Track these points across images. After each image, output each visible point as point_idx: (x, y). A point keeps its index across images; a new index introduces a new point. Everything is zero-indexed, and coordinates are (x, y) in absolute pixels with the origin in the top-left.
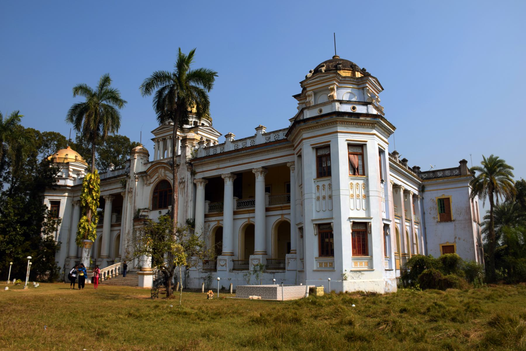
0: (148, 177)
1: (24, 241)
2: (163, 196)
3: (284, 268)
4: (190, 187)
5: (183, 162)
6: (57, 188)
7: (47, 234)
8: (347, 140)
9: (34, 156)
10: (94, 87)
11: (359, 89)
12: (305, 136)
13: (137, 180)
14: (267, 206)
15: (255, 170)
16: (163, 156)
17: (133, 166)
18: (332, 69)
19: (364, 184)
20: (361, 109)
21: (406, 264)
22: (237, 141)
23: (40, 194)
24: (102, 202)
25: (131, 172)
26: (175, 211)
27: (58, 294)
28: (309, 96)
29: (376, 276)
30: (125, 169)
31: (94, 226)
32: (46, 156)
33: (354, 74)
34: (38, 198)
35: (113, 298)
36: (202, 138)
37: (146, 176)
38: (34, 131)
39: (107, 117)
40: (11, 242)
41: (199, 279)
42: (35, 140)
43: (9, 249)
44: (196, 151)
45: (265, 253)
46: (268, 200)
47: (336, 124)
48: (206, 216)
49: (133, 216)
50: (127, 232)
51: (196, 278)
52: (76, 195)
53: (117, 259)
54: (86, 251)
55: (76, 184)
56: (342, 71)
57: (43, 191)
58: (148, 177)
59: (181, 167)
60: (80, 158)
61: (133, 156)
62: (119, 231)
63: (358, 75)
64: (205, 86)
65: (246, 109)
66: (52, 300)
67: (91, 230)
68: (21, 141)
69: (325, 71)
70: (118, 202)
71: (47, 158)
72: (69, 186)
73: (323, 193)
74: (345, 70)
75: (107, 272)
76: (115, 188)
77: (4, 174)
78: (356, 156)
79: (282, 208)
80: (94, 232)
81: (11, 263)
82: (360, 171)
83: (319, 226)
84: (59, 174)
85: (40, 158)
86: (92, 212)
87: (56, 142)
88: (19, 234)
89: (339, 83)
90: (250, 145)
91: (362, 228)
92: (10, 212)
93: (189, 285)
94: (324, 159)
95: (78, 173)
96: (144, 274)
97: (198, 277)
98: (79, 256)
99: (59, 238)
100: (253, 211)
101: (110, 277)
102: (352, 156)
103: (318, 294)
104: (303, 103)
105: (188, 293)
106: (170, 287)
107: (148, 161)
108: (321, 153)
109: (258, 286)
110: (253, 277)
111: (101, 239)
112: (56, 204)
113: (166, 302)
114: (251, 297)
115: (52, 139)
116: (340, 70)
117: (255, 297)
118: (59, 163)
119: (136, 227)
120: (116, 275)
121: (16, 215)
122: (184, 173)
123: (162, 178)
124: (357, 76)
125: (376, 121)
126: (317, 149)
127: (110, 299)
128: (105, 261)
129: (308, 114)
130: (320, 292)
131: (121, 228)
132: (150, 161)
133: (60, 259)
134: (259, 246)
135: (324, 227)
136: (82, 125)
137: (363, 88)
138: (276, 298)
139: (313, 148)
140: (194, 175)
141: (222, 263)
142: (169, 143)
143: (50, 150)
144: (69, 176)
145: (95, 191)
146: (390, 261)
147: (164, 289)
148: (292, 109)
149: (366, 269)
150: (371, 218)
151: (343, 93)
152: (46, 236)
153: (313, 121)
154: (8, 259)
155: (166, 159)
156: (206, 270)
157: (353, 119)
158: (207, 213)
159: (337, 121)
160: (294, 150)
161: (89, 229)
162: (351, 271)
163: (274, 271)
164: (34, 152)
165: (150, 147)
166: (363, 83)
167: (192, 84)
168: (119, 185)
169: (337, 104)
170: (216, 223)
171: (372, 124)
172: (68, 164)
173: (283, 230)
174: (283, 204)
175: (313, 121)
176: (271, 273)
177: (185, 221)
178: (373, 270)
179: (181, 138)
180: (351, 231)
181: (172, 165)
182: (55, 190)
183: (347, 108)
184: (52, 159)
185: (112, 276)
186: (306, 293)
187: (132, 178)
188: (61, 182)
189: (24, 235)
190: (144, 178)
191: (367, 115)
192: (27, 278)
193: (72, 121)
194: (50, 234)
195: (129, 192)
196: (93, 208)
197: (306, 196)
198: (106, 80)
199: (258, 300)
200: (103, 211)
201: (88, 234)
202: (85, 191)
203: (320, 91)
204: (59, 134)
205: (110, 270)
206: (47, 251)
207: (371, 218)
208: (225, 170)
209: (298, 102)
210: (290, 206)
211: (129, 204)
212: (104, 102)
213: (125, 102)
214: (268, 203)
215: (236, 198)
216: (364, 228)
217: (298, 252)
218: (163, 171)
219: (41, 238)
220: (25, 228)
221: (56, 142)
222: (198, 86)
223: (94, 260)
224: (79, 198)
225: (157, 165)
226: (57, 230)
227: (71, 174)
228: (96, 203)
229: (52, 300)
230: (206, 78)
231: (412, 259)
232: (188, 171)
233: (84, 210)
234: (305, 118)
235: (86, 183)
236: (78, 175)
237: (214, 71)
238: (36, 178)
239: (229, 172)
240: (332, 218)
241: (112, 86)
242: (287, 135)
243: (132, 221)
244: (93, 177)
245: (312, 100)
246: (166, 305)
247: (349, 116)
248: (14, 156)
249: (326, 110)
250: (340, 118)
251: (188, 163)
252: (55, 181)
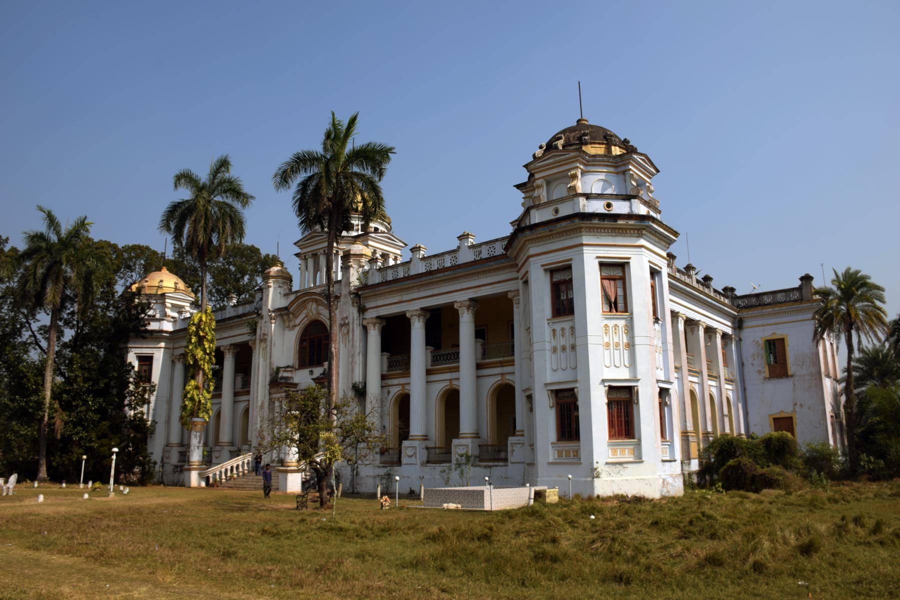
0: (291, 316)
1: (99, 422)
2: (315, 346)
3: (506, 460)
4: (358, 331)
5: (344, 291)
6: (148, 335)
7: (135, 409)
8: (598, 257)
9: (110, 284)
10: (203, 175)
11: (617, 173)
12: (532, 251)
13: (273, 321)
14: (479, 361)
15: (459, 304)
16: (315, 282)
17: (267, 299)
18: (574, 143)
19: (626, 326)
20: (620, 207)
21: (706, 450)
22: (429, 257)
23: (122, 346)
24: (219, 355)
25: (264, 307)
26: (334, 372)
27: (159, 504)
28: (539, 187)
29: (649, 471)
30: (255, 304)
31: (208, 396)
32: (128, 284)
33: (609, 150)
34: (118, 352)
35: (241, 510)
36: (374, 253)
37: (288, 315)
38: (108, 244)
39: (224, 223)
40: (79, 423)
41: (374, 477)
42: (111, 260)
43: (77, 434)
44: (366, 273)
45: (477, 435)
46: (480, 351)
47: (581, 232)
48: (383, 377)
49: (268, 379)
50: (259, 404)
51: (370, 477)
52: (177, 345)
53: (245, 447)
54: (196, 436)
55: (177, 328)
56: (589, 146)
57: (127, 342)
58: (291, 316)
59: (342, 299)
60: (181, 285)
61: (267, 283)
62: (246, 403)
63: (616, 151)
64: (374, 170)
65: (442, 205)
66: (154, 513)
67: (203, 401)
68: (91, 263)
69: (563, 147)
70: (244, 357)
71: (130, 287)
72: (166, 332)
73: (562, 342)
74: (594, 143)
75: (229, 468)
76: (240, 335)
77: (66, 316)
78: (612, 282)
79: (501, 364)
80: (209, 405)
81: (85, 457)
82: (621, 305)
84: (151, 313)
85: (119, 289)
86: (205, 374)
87: (142, 262)
88: (91, 410)
89: (585, 165)
90: (449, 265)
91: (624, 396)
92: (76, 376)
93: (358, 487)
94: (563, 287)
95: (179, 309)
96: (287, 472)
97: (372, 474)
98: (186, 442)
99: (154, 416)
100: (457, 369)
101: (235, 476)
102: (606, 282)
103: (548, 500)
104: (530, 197)
105: (356, 500)
106: (325, 492)
107: (291, 290)
109: (459, 488)
110: (455, 475)
111: (218, 415)
112: (146, 361)
113: (317, 514)
114: (445, 505)
115: (138, 257)
116: (586, 144)
117: (452, 506)
118: (150, 296)
119: (274, 396)
120: (243, 472)
121: (85, 380)
122: (347, 310)
123: (314, 318)
124: (614, 154)
125: (640, 226)
126: (552, 272)
127: (237, 511)
128: (226, 450)
129: (537, 217)
130: (552, 496)
131: (251, 397)
132: (294, 289)
133: (156, 448)
134: (466, 424)
135: (565, 394)
136: (185, 236)
137: (624, 173)
138: (483, 507)
139: (546, 270)
140: (363, 313)
141: (410, 452)
142: (323, 261)
143: (134, 274)
144: (165, 315)
145: (208, 341)
146: (672, 446)
147: (318, 494)
148: (515, 206)
149: (631, 460)
150: (638, 380)
151: (592, 182)
152: (132, 413)
153: (545, 228)
154: (75, 449)
155: (319, 286)
156: (384, 462)
157: (607, 223)
158: (385, 373)
159: (582, 228)
160: (518, 272)
161: (200, 401)
162: (607, 463)
163: (491, 464)
164: (111, 279)
165: (293, 266)
166: (624, 165)
167: (356, 169)
168: (246, 330)
169: (582, 201)
170: (400, 388)
171: (638, 230)
172: (163, 295)
173: (504, 397)
174: (503, 357)
175: (545, 228)
176: (485, 467)
177: (351, 386)
178: (642, 462)
179: (341, 253)
180: (606, 401)
181: (329, 297)
182: (144, 338)
183: (597, 207)
184: (139, 289)
185: (238, 474)
186: (530, 498)
187: (266, 318)
188: (154, 326)
189: (97, 411)
190: (285, 317)
191: (630, 216)
192: (112, 480)
193: (168, 229)
194: (140, 409)
195: (261, 341)
196: (206, 367)
197: (536, 347)
198: (224, 164)
199: (456, 511)
200: (222, 369)
201: (199, 409)
202: (193, 341)
203: (557, 179)
204: (147, 248)
205: (235, 465)
206: (135, 436)
207: (638, 380)
208: (412, 304)
209: (523, 195)
210: (513, 361)
211: (261, 360)
212: (218, 198)
213: (252, 197)
214: (480, 356)
215: (431, 348)
216: (628, 396)
217: (526, 433)
218: (314, 306)
219: (125, 417)
220: (101, 400)
221: (142, 262)
222: (363, 172)
223: (208, 449)
224: (182, 351)
225: (304, 297)
226: (149, 403)
227: (169, 312)
228: (210, 358)
229: (154, 513)
230: (375, 157)
231: (714, 442)
232: (353, 306)
233: (191, 370)
234: (532, 223)
235: (194, 328)
236: (180, 313)
237: (389, 146)
238: (115, 321)
239: (418, 308)
240: (576, 381)
241: (234, 173)
242: (506, 248)
243: (268, 387)
244: (204, 319)
245: (543, 194)
246: (315, 519)
247: (600, 220)
248: (81, 288)
249: (565, 210)
250: (586, 223)
251: (353, 293)
252: (145, 325)
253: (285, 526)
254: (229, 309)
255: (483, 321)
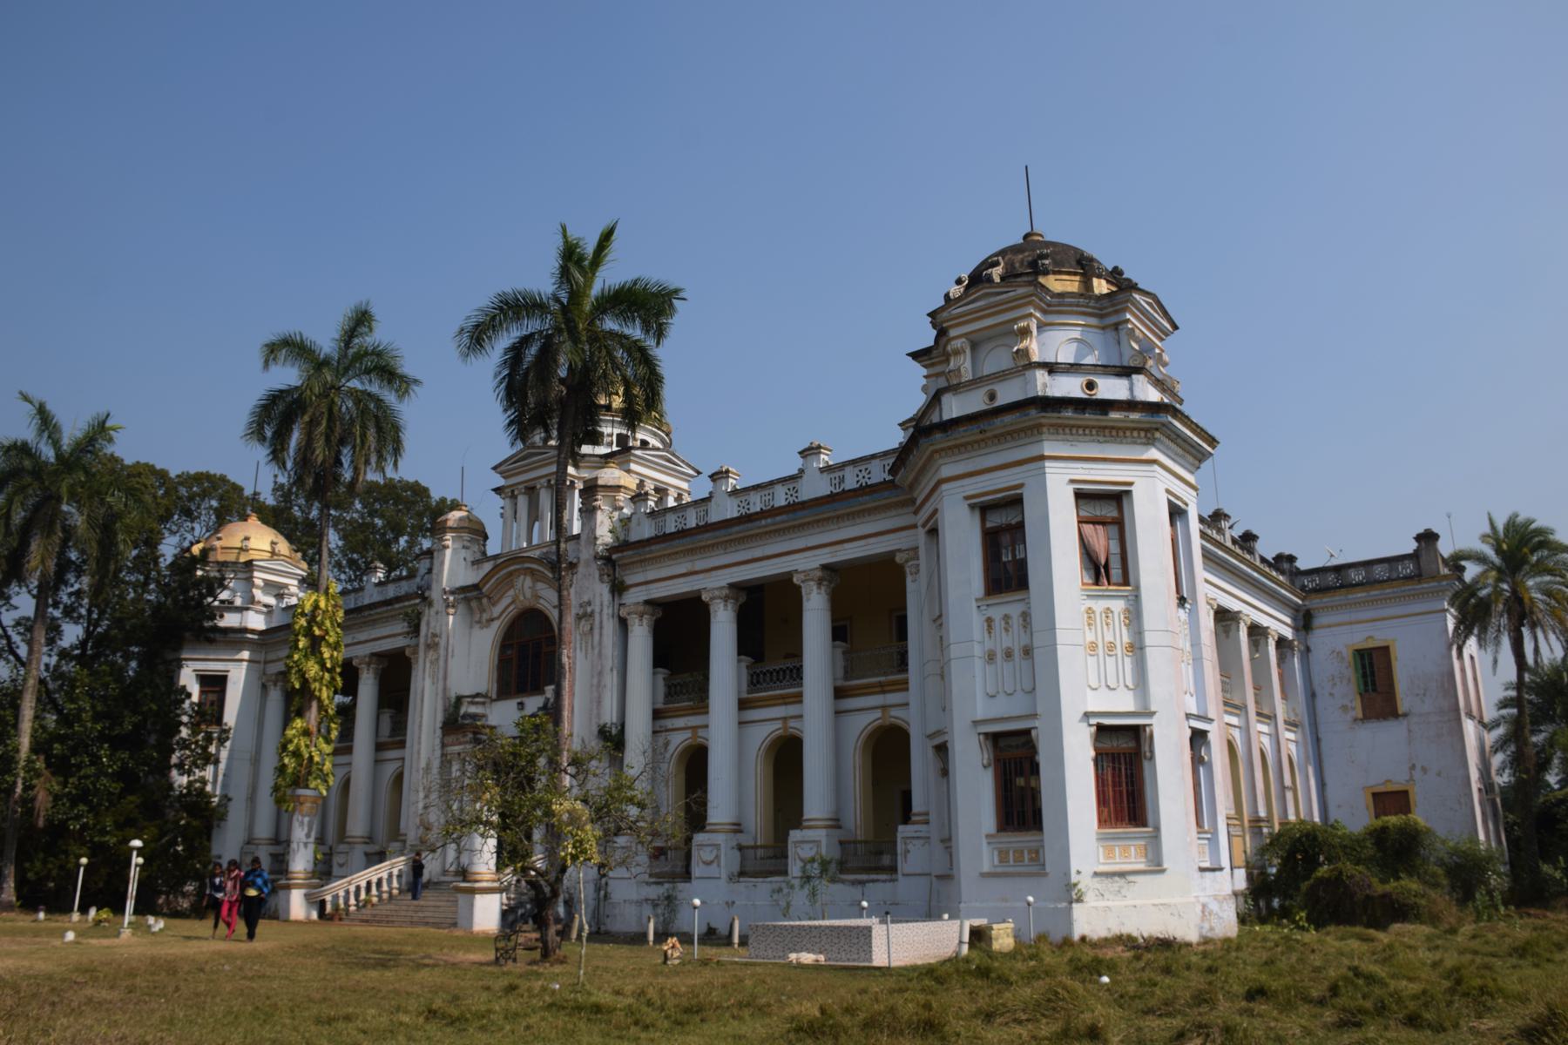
0: (485, 601)
1: (121, 796)
2: (529, 658)
3: (893, 869)
4: (610, 627)
5: (586, 554)
6: (218, 636)
7: (189, 773)
8: (1072, 481)
9: (152, 542)
10: (326, 340)
11: (1103, 328)
12: (947, 471)
13: (451, 611)
14: (840, 683)
15: (802, 576)
16: (530, 540)
17: (441, 571)
19: (1127, 610)
20: (1111, 389)
21: (1262, 851)
22: (746, 490)
23: (170, 656)
24: (349, 676)
25: (434, 586)
26: (566, 702)
27: (219, 953)
28: (957, 352)
29: (1174, 889)
30: (418, 580)
31: (328, 749)
32: (186, 544)
33: (1087, 285)
34: (161, 668)
35: (383, 964)
36: (641, 484)
37: (479, 599)
38: (151, 469)
39: (364, 427)
40: (82, 797)
41: (639, 903)
42: (155, 497)
43: (78, 817)
44: (626, 522)
45: (835, 823)
46: (840, 663)
47: (1041, 433)
48: (657, 715)
49: (440, 718)
50: (423, 764)
51: (631, 902)
52: (271, 656)
53: (396, 845)
54: (302, 823)
55: (273, 625)
56: (1051, 277)
57: (178, 648)
58: (485, 601)
59: (581, 569)
60: (284, 547)
61: (441, 540)
62: (399, 764)
63: (1101, 287)
64: (646, 328)
65: (773, 393)
66: (202, 970)
67: (317, 759)
68: (115, 499)
69: (1003, 279)
70: (395, 678)
71: (188, 550)
72: (253, 631)
73: (1007, 641)
74: (1060, 273)
75: (363, 884)
76: (389, 635)
77: (65, 599)
78: (1100, 528)
79: (883, 689)
80: (328, 766)
81: (84, 860)
82: (1116, 572)
83: (995, 739)
84: (224, 595)
85: (168, 549)
86: (321, 707)
87: (214, 503)
88: (106, 775)
89: (1044, 312)
90: (783, 503)
91: (1125, 744)
92: (81, 710)
93: (608, 921)
94: (1005, 539)
95: (279, 591)
96: (473, 891)
97: (634, 897)
98: (283, 837)
99: (224, 786)
100: (798, 698)
101: (375, 900)
102: (1088, 529)
103: (996, 946)
104: (937, 375)
105: (606, 947)
106: (553, 929)
107: (484, 553)
108: (995, 520)
109: (816, 923)
110: (800, 897)
111: (346, 786)
112: (214, 684)
113: (538, 975)
114: (793, 956)
115: (205, 495)
116: (1046, 273)
117: (807, 958)
118: (223, 565)
119: (450, 749)
120: (390, 893)
121: (97, 717)
122: (590, 588)
123: (527, 604)
124: (1097, 291)
125: (1157, 423)
126: (984, 509)
127: (374, 967)
128: (359, 852)
129: (954, 407)
130: (1003, 938)
131: (407, 753)
132: (489, 553)
133: (228, 845)
134: (816, 799)
135: (1014, 741)
136: (292, 452)
137: (1116, 327)
138: (870, 960)
139: (972, 507)
140: (620, 595)
141: (707, 855)
142: (546, 500)
143: (197, 526)
144: (252, 600)
145: (329, 645)
146: (1213, 841)
147: (535, 935)
148: (907, 392)
149: (1142, 867)
150: (1151, 714)
151: (1058, 342)
152: (184, 780)
154: (74, 848)
155: (538, 546)
156: (657, 875)
157: (1089, 417)
158: (660, 706)
159: (1041, 425)
160: (916, 513)
161: (311, 758)
162: (1096, 874)
163: (864, 877)
164: (152, 531)
165: (490, 511)
166: (1117, 312)
167: (610, 324)
168: (401, 627)
169: (1041, 376)
170: (688, 734)
171: (1147, 430)
172: (249, 565)
173: (888, 752)
174: (885, 674)
176: (853, 883)
177: (595, 730)
178: (1163, 871)
179: (580, 485)
180: (1093, 753)
181: (557, 565)
182: (211, 641)
183: (1070, 387)
184: (205, 552)
185: (380, 897)
186: (961, 942)
187: (438, 605)
188: (230, 620)
189: (117, 776)
190: (474, 604)
191: (1131, 405)
192: (130, 905)
193: (262, 439)
194: (198, 773)
195: (428, 647)
196: (325, 694)
197: (954, 651)
198: (362, 320)
199: (816, 967)
200: (354, 705)
201: (309, 773)
202: (301, 645)
203: (990, 339)
204: (223, 479)
205: (374, 880)
206: (188, 824)
207: (1151, 714)
208: (713, 578)
209: (924, 372)
210: (906, 682)
211: (428, 682)
212: (355, 384)
213: (416, 381)
214: (840, 673)
215: (747, 660)
216: (1132, 744)
217: (932, 818)
218: (528, 582)
219: (171, 787)
220: (126, 755)
221: (214, 503)
222: (627, 331)
223: (325, 849)
224: (281, 667)
225: (510, 565)
226: (217, 762)
227: (258, 594)
228: (333, 679)
229: (202, 970)
230: (650, 304)
231: (1280, 835)
232: (602, 581)
233: (297, 700)
234: (946, 417)
235: (303, 622)
236: (280, 597)
237: (673, 284)
238: (158, 608)
239: (724, 583)
240: (1034, 716)
241: (380, 336)
242: (893, 470)
243: (439, 732)
244: (322, 604)
245: (965, 366)
246: (537, 985)
247: (1076, 410)
248: (94, 544)
249: (1008, 393)
250: (1051, 417)
251: (602, 558)
252: (213, 618)
253: (477, 1002)
254: (369, 589)
255: (845, 605)
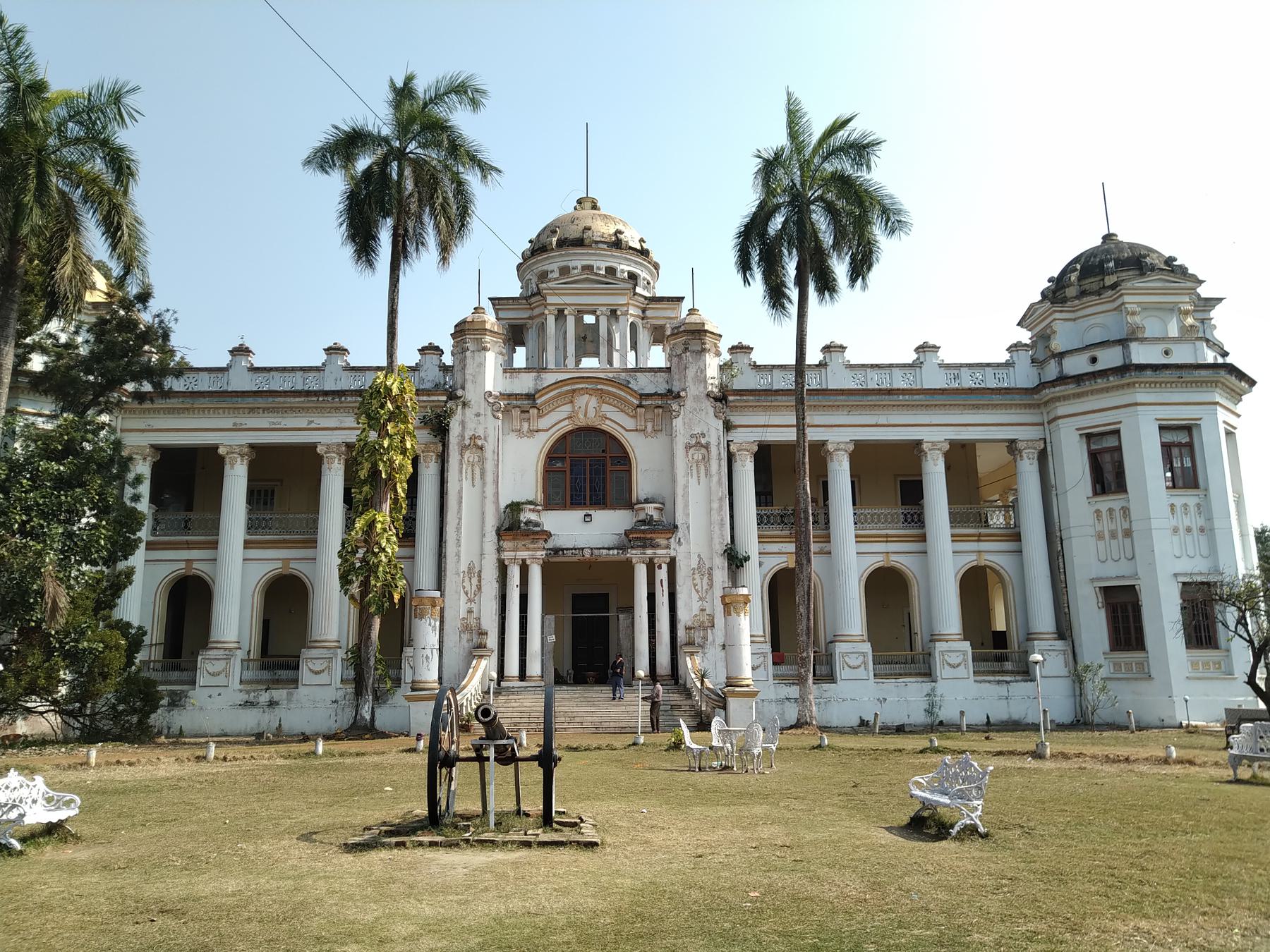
83: (1107, 591)
